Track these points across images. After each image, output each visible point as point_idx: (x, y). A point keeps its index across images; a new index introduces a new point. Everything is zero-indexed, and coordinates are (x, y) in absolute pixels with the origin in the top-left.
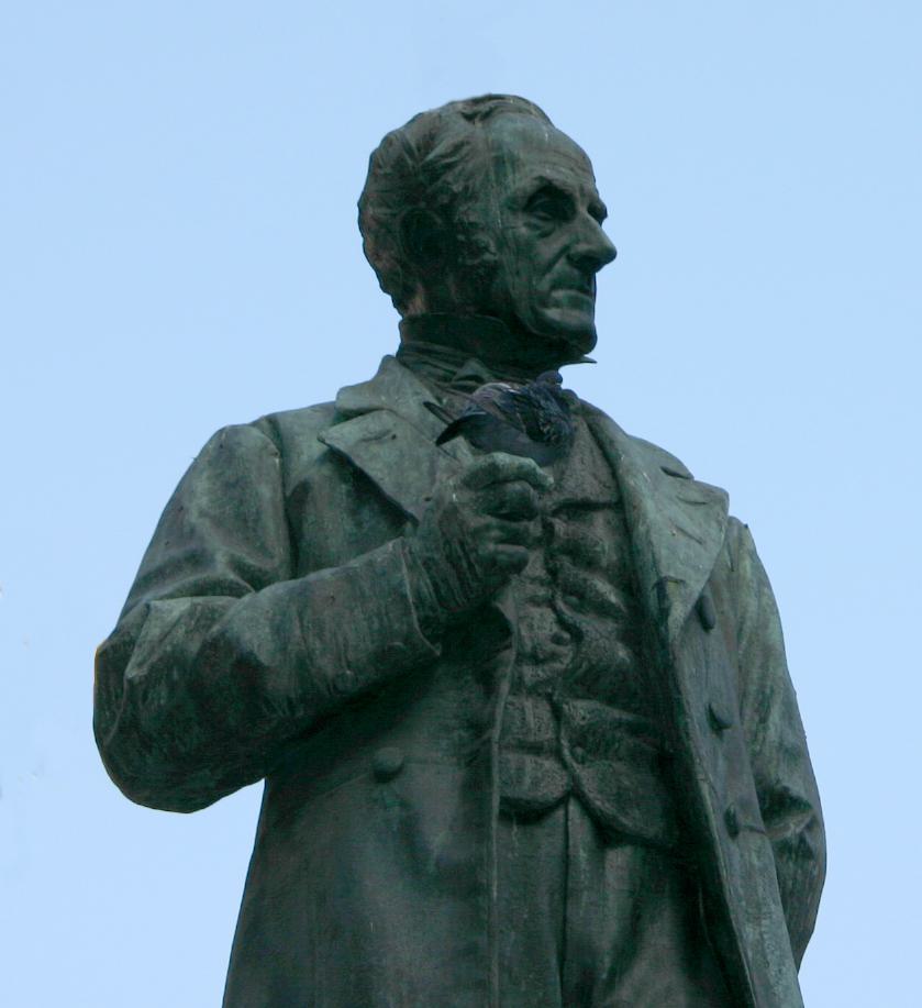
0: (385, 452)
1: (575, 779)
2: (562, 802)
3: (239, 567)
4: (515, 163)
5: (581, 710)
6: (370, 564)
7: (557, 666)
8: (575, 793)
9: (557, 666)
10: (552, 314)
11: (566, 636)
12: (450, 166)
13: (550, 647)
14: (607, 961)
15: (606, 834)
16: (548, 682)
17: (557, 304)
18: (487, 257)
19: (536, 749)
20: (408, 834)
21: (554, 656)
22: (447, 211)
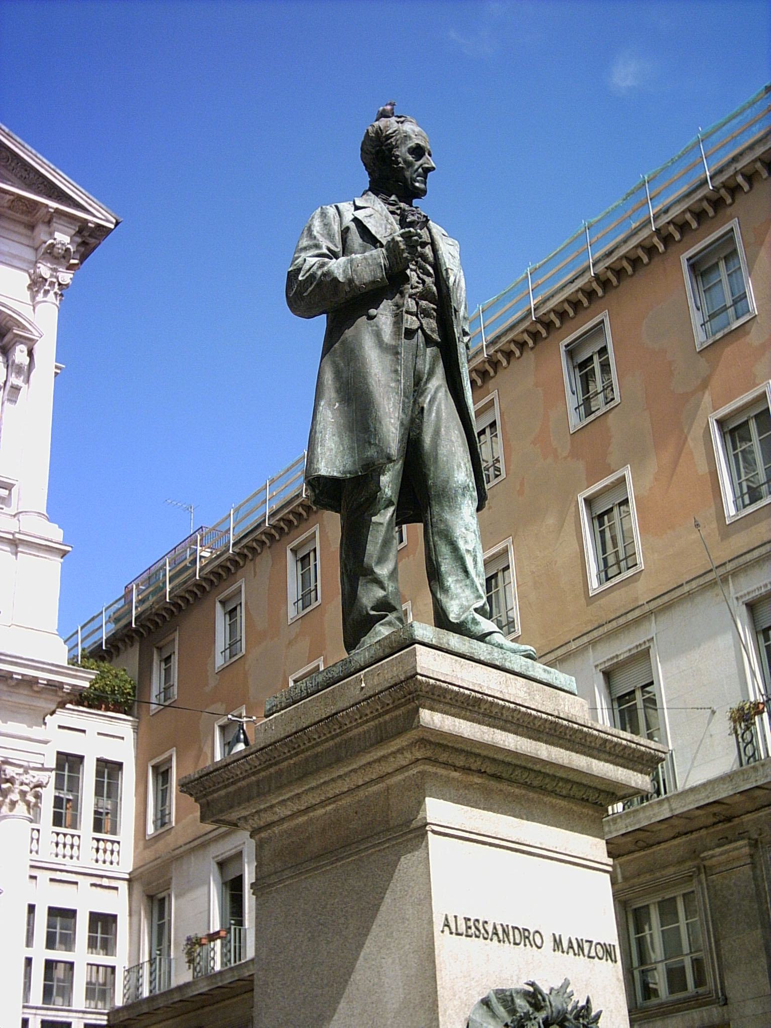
0: (372, 220)
1: (421, 324)
2: (417, 330)
3: (329, 249)
4: (410, 138)
5: (424, 303)
6: (371, 255)
7: (417, 290)
8: (421, 327)
9: (417, 290)
10: (417, 184)
11: (420, 281)
12: (393, 137)
13: (416, 284)
14: (426, 376)
15: (429, 341)
16: (415, 294)
17: (418, 182)
18: (400, 165)
19: (411, 314)
20: (378, 335)
21: (417, 287)
22: (390, 150)
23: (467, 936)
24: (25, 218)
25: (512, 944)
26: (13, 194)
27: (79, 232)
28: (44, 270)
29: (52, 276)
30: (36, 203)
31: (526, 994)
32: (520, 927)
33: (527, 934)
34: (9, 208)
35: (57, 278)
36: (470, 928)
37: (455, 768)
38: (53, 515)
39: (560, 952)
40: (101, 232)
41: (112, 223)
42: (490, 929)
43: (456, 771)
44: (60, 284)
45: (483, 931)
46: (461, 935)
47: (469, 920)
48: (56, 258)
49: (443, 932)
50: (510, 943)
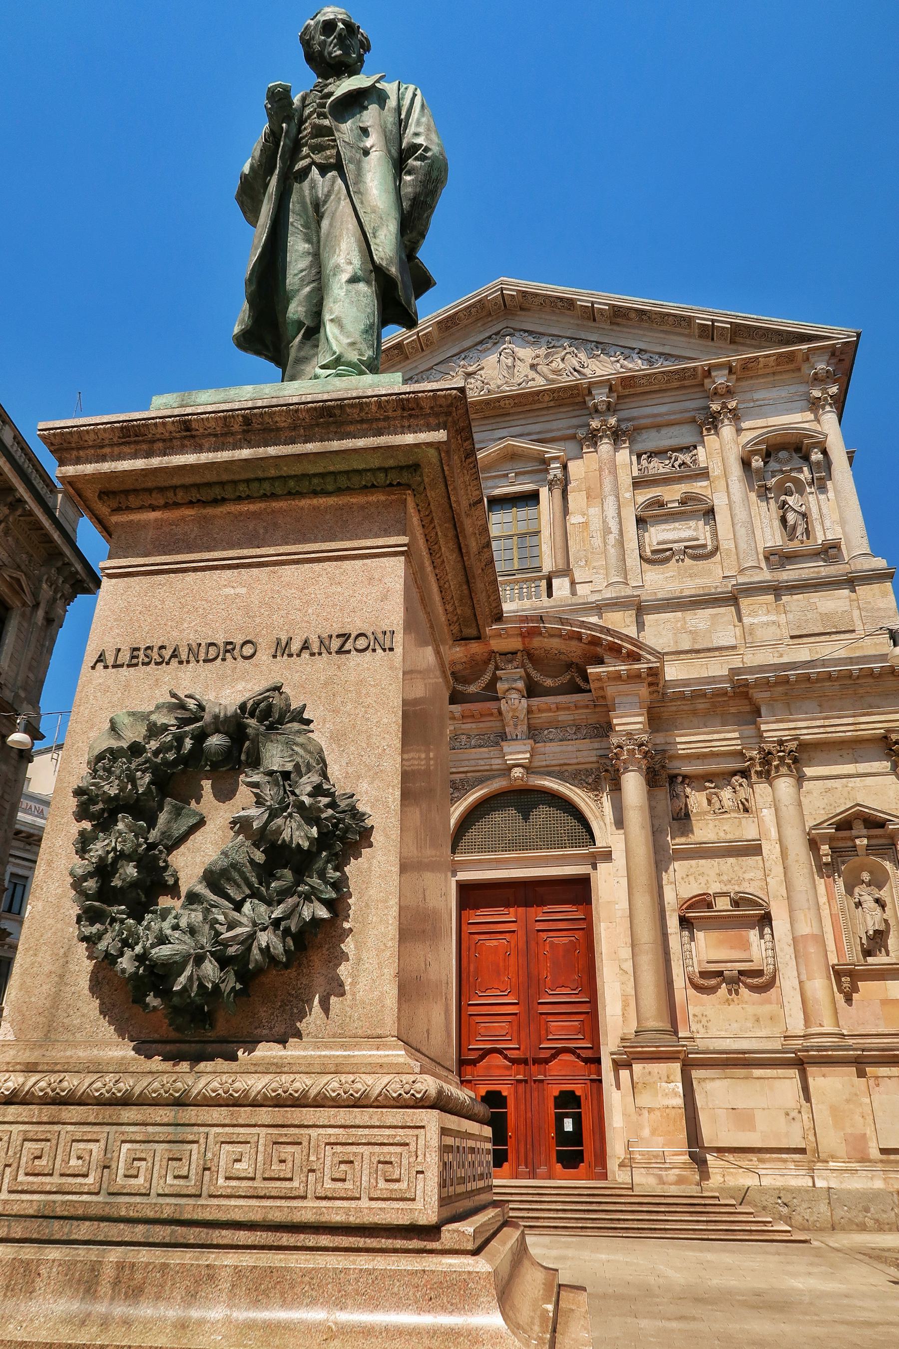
23: (129, 666)
24: (791, 366)
25: (201, 662)
26: (774, 354)
27: (833, 354)
28: (816, 393)
29: (823, 394)
30: (793, 352)
31: (172, 708)
32: (220, 642)
33: (229, 647)
34: (778, 365)
35: (828, 393)
36: (137, 657)
37: (154, 508)
38: (876, 552)
39: (285, 657)
40: (851, 348)
41: (853, 336)
42: (167, 654)
43: (154, 510)
44: (831, 397)
45: (156, 656)
46: (122, 666)
47: (138, 649)
48: (822, 381)
49: (93, 668)
50: (198, 661)
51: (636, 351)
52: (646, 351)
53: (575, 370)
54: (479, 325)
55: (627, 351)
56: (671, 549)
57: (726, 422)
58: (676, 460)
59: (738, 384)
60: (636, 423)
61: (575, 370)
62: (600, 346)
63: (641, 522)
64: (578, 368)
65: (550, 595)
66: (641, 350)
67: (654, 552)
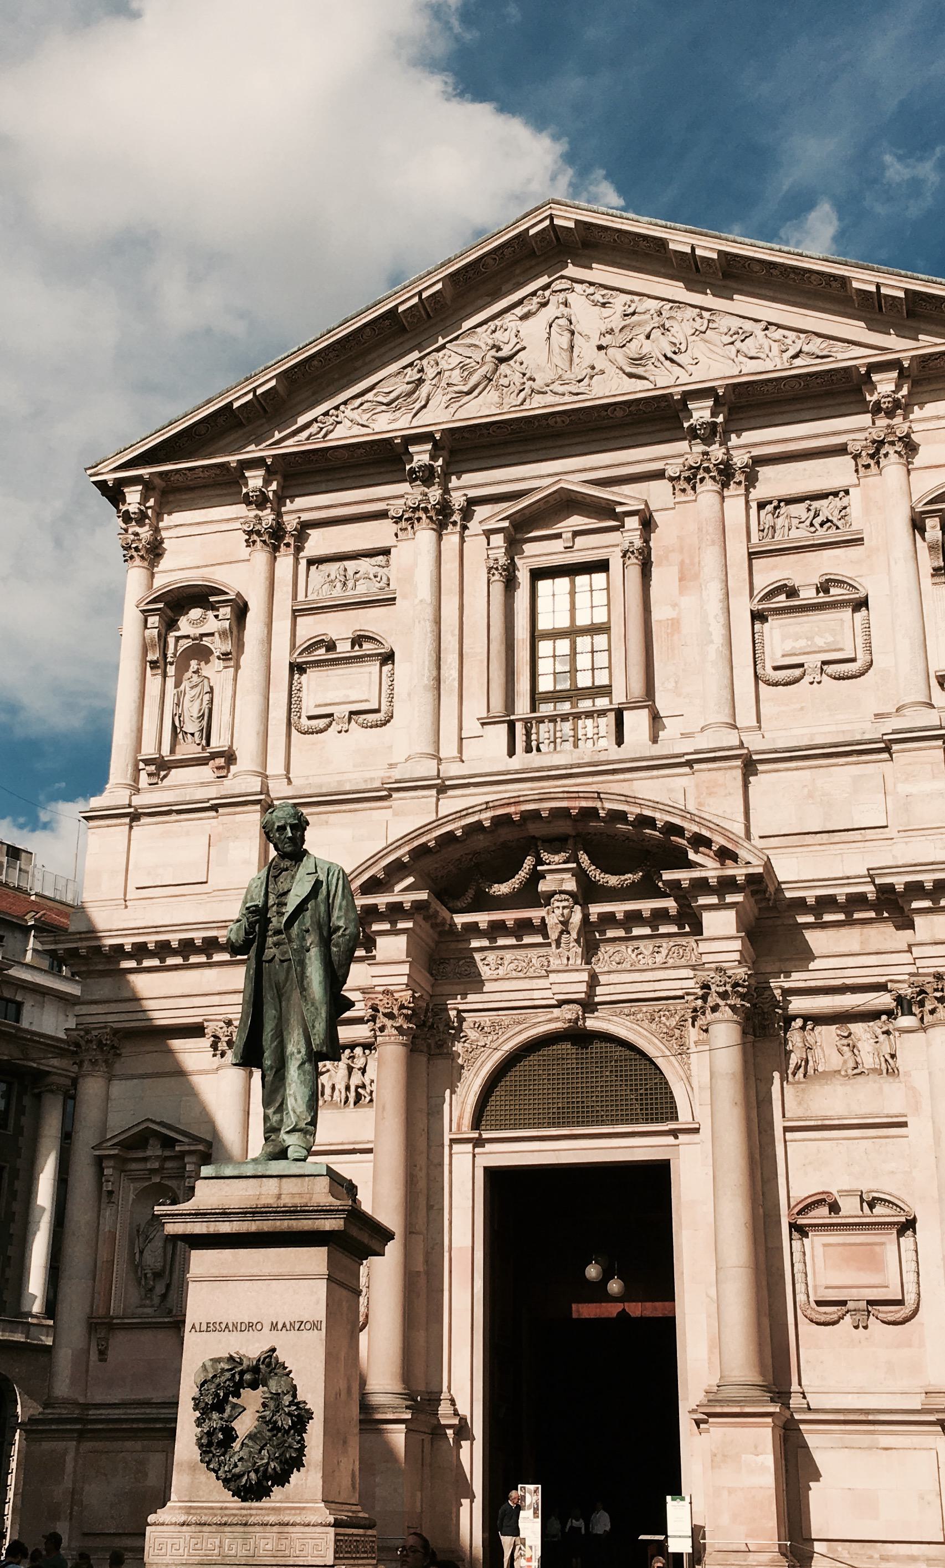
51: (763, 325)
52: (779, 326)
53: (666, 358)
54: (518, 271)
55: (748, 326)
56: (802, 665)
57: (893, 457)
58: (816, 515)
59: (915, 390)
60: (756, 452)
61: (665, 356)
62: (706, 314)
63: (758, 617)
64: (670, 355)
65: (620, 741)
66: (770, 324)
67: (776, 668)
